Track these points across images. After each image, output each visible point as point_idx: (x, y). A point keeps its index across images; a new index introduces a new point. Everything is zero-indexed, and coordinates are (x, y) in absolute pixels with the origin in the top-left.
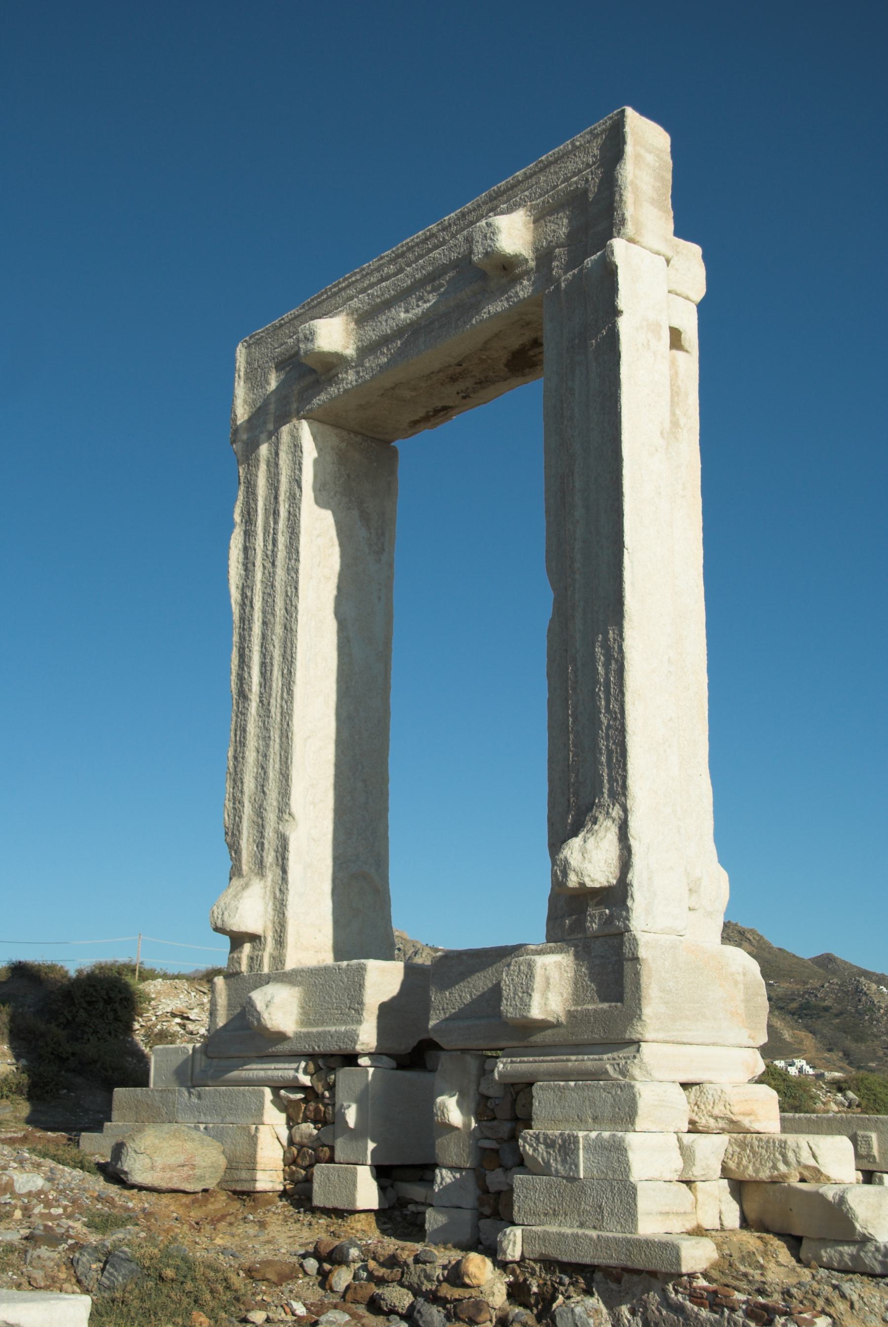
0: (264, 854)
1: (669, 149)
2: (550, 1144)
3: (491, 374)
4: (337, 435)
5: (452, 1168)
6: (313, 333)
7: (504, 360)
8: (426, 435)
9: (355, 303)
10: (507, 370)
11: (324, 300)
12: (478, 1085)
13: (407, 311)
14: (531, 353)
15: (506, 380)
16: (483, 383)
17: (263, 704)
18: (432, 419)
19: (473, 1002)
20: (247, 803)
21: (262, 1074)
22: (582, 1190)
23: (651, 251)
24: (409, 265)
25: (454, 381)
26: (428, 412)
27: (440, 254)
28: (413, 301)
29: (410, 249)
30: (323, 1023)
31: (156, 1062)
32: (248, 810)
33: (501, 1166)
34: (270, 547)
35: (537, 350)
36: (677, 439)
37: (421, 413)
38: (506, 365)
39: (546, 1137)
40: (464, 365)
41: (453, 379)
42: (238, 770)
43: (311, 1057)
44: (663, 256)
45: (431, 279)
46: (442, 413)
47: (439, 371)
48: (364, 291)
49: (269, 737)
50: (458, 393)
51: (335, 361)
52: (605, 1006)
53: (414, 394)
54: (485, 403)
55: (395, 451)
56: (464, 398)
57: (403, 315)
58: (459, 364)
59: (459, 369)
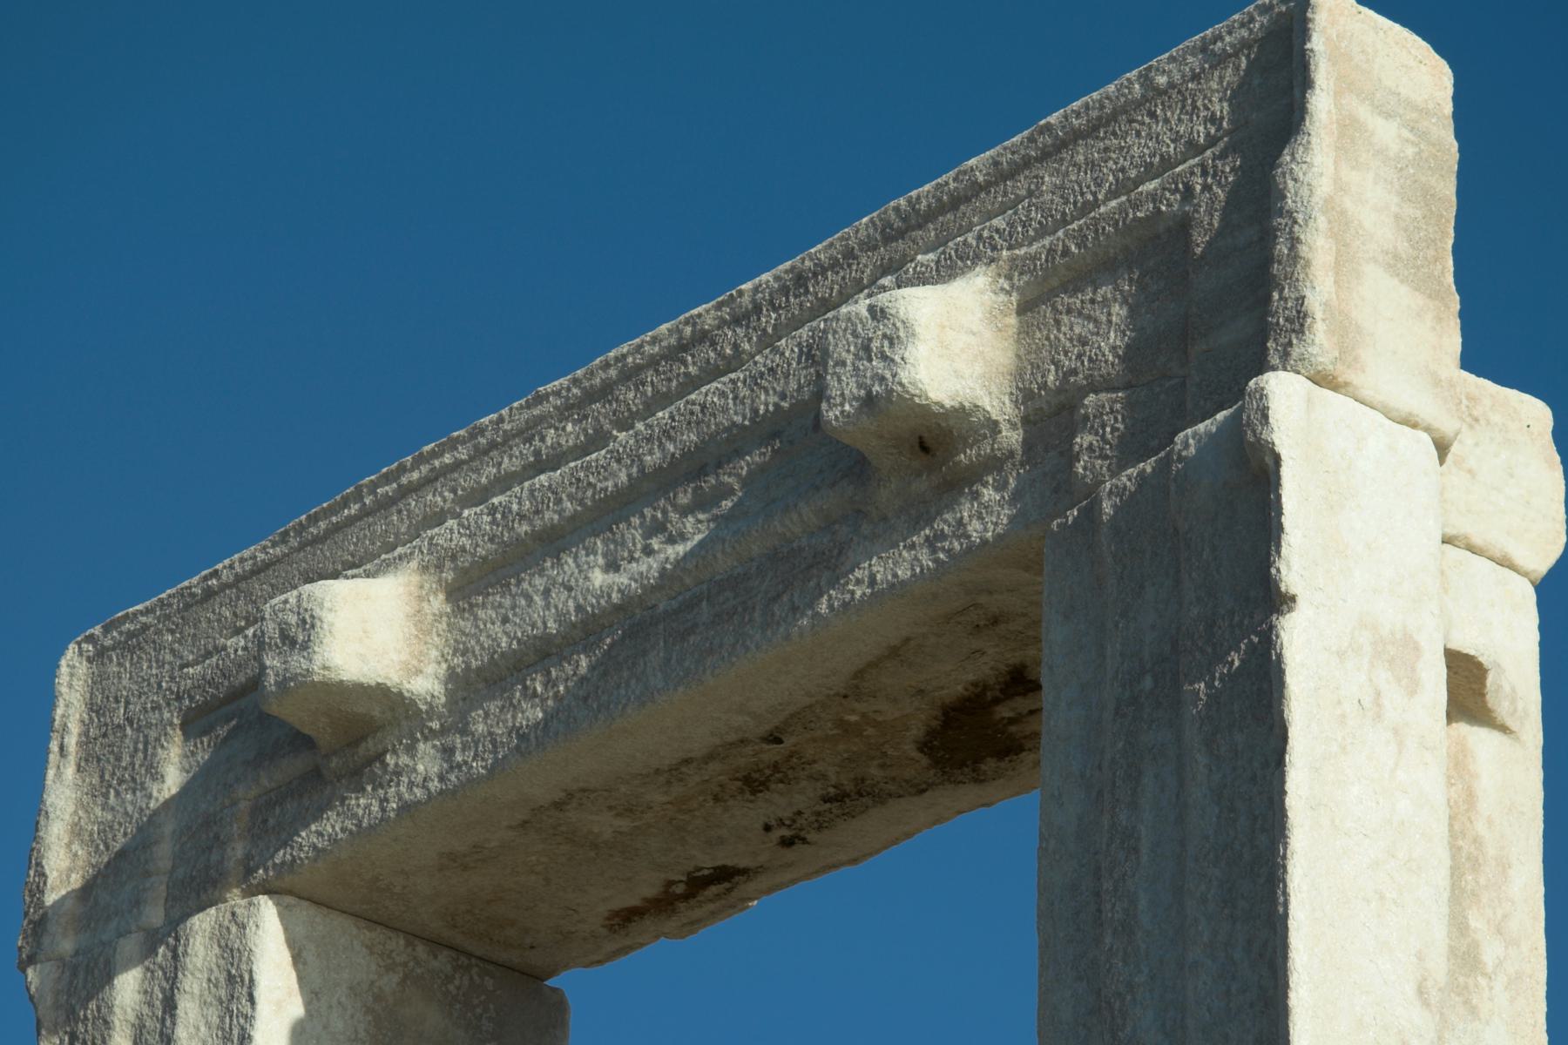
1: (1448, 108)
3: (874, 771)
4: (370, 948)
6: (308, 623)
7: (917, 731)
8: (661, 957)
9: (448, 534)
10: (925, 761)
11: (351, 521)
13: (612, 566)
14: (1004, 711)
15: (923, 791)
16: (847, 799)
18: (682, 906)
23: (1388, 413)
24: (625, 425)
25: (754, 792)
26: (670, 883)
27: (723, 395)
29: (630, 375)
35: (1021, 704)
36: (1473, 1011)
37: (648, 887)
38: (925, 747)
40: (789, 741)
41: (753, 784)
44: (1427, 429)
45: (693, 469)
46: (714, 889)
47: (710, 757)
48: (479, 496)
50: (767, 828)
51: (376, 713)
53: (624, 824)
54: (854, 861)
55: (557, 1007)
56: (787, 843)
57: (598, 578)
58: (774, 739)
59: (772, 753)
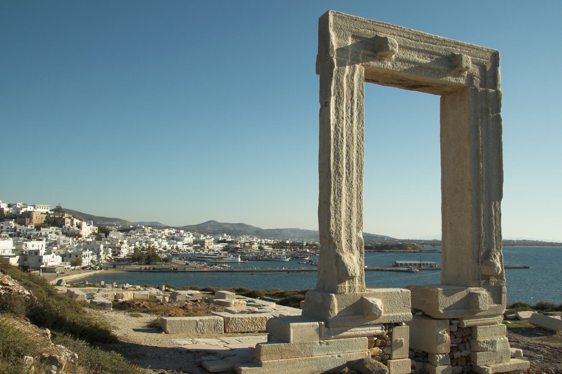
0: (352, 245)
2: (488, 343)
5: (442, 354)
12: (450, 328)
17: (348, 181)
19: (454, 304)
20: (343, 222)
21: (364, 332)
22: (497, 354)
28: (421, 56)
30: (392, 312)
31: (293, 332)
32: (343, 226)
33: (457, 351)
34: (350, 114)
39: (487, 341)
42: (338, 206)
43: (384, 324)
45: (431, 53)
49: (352, 196)
52: (496, 305)
